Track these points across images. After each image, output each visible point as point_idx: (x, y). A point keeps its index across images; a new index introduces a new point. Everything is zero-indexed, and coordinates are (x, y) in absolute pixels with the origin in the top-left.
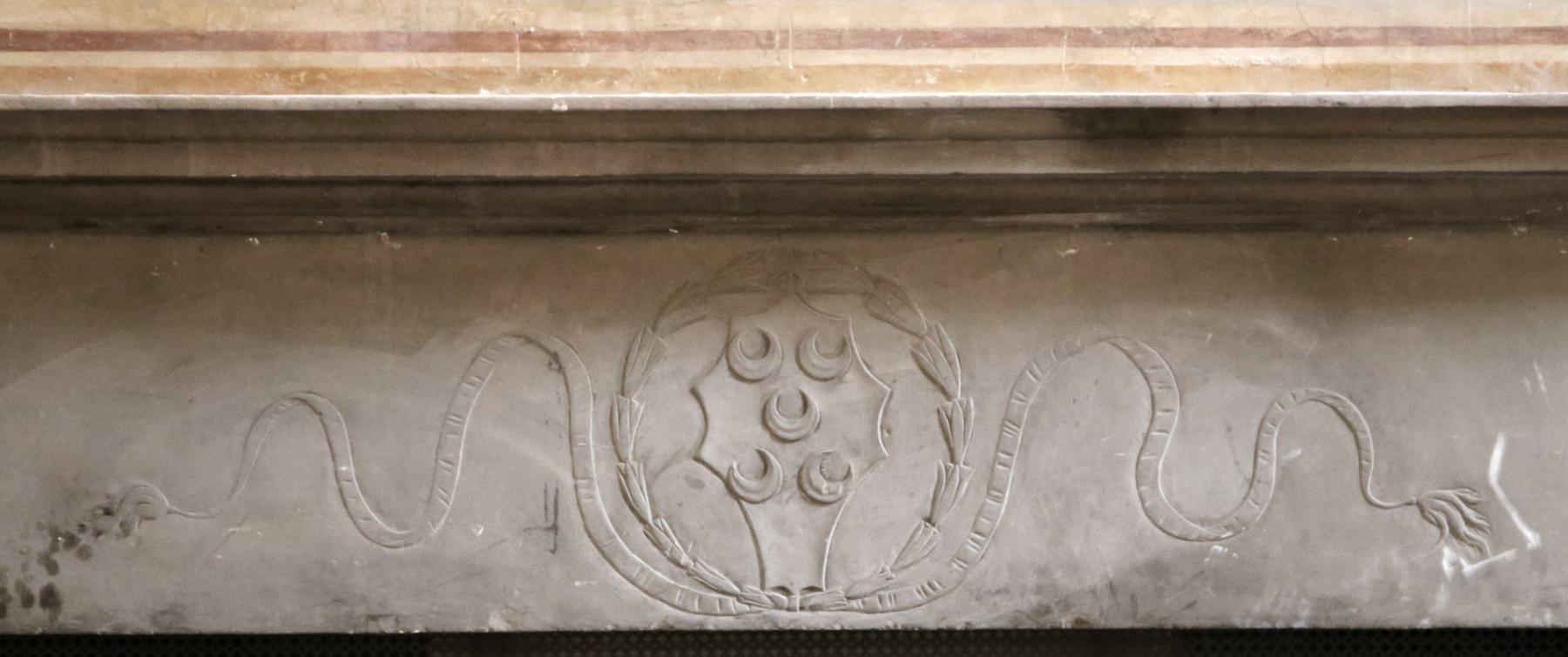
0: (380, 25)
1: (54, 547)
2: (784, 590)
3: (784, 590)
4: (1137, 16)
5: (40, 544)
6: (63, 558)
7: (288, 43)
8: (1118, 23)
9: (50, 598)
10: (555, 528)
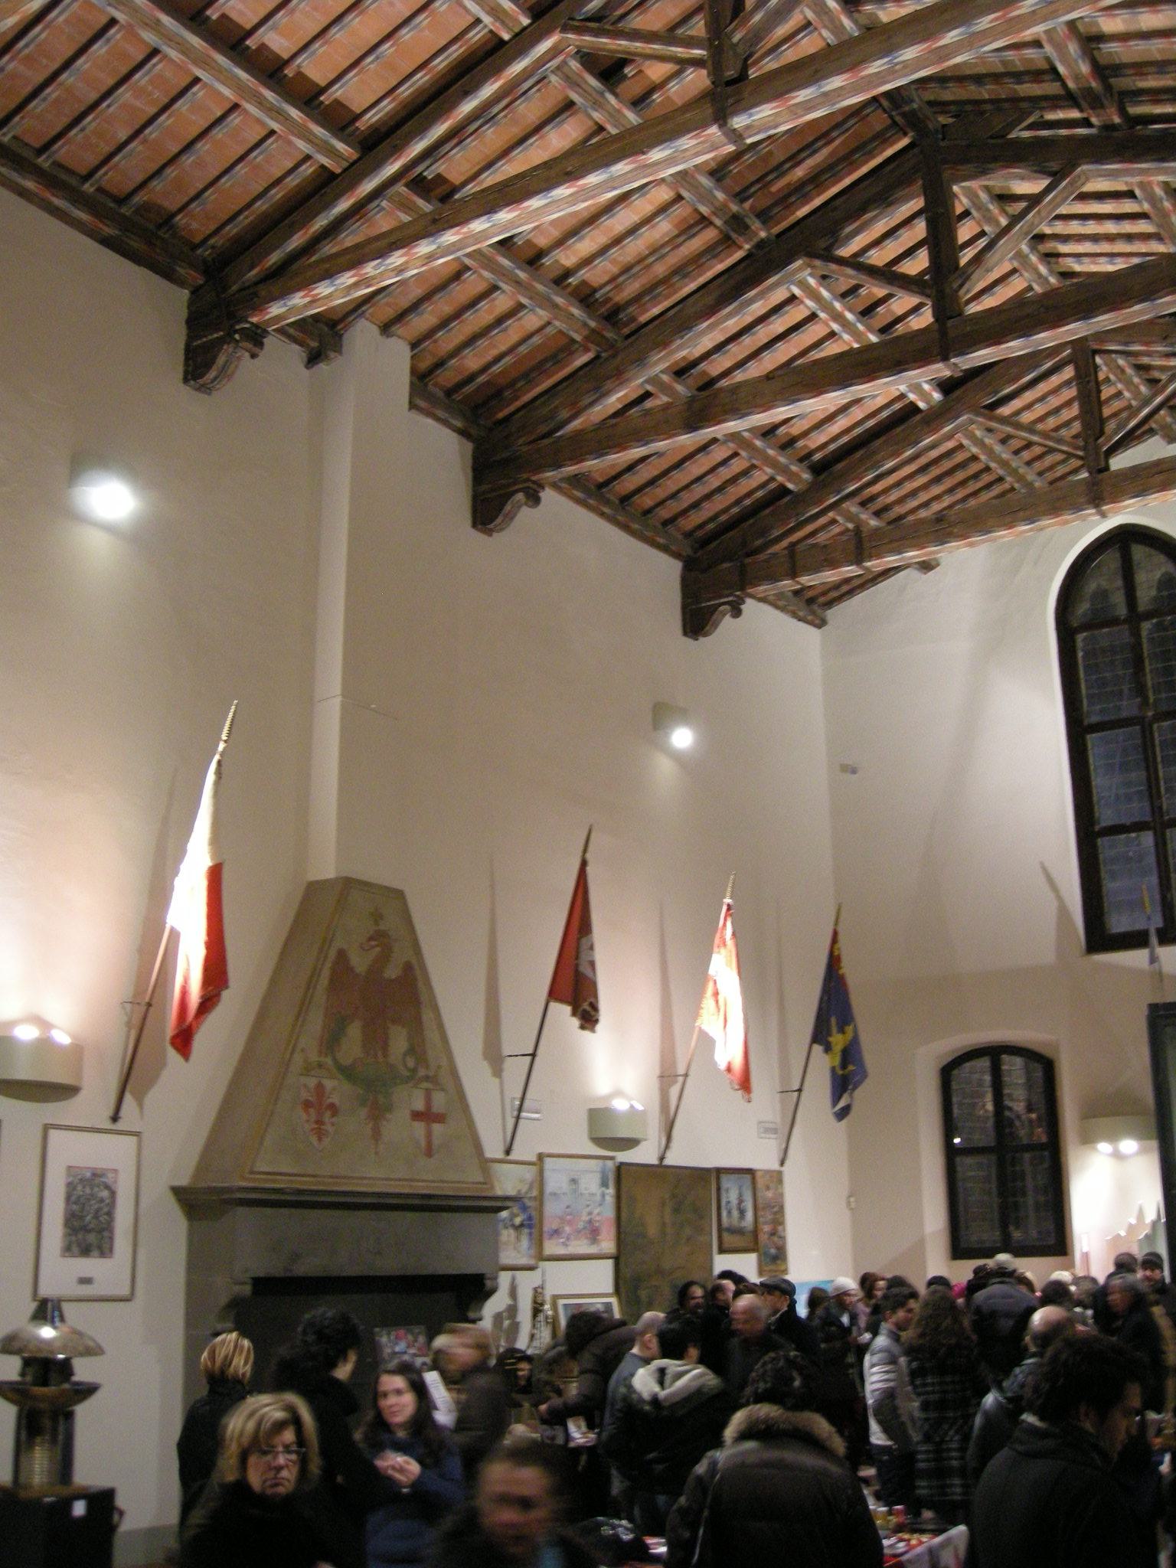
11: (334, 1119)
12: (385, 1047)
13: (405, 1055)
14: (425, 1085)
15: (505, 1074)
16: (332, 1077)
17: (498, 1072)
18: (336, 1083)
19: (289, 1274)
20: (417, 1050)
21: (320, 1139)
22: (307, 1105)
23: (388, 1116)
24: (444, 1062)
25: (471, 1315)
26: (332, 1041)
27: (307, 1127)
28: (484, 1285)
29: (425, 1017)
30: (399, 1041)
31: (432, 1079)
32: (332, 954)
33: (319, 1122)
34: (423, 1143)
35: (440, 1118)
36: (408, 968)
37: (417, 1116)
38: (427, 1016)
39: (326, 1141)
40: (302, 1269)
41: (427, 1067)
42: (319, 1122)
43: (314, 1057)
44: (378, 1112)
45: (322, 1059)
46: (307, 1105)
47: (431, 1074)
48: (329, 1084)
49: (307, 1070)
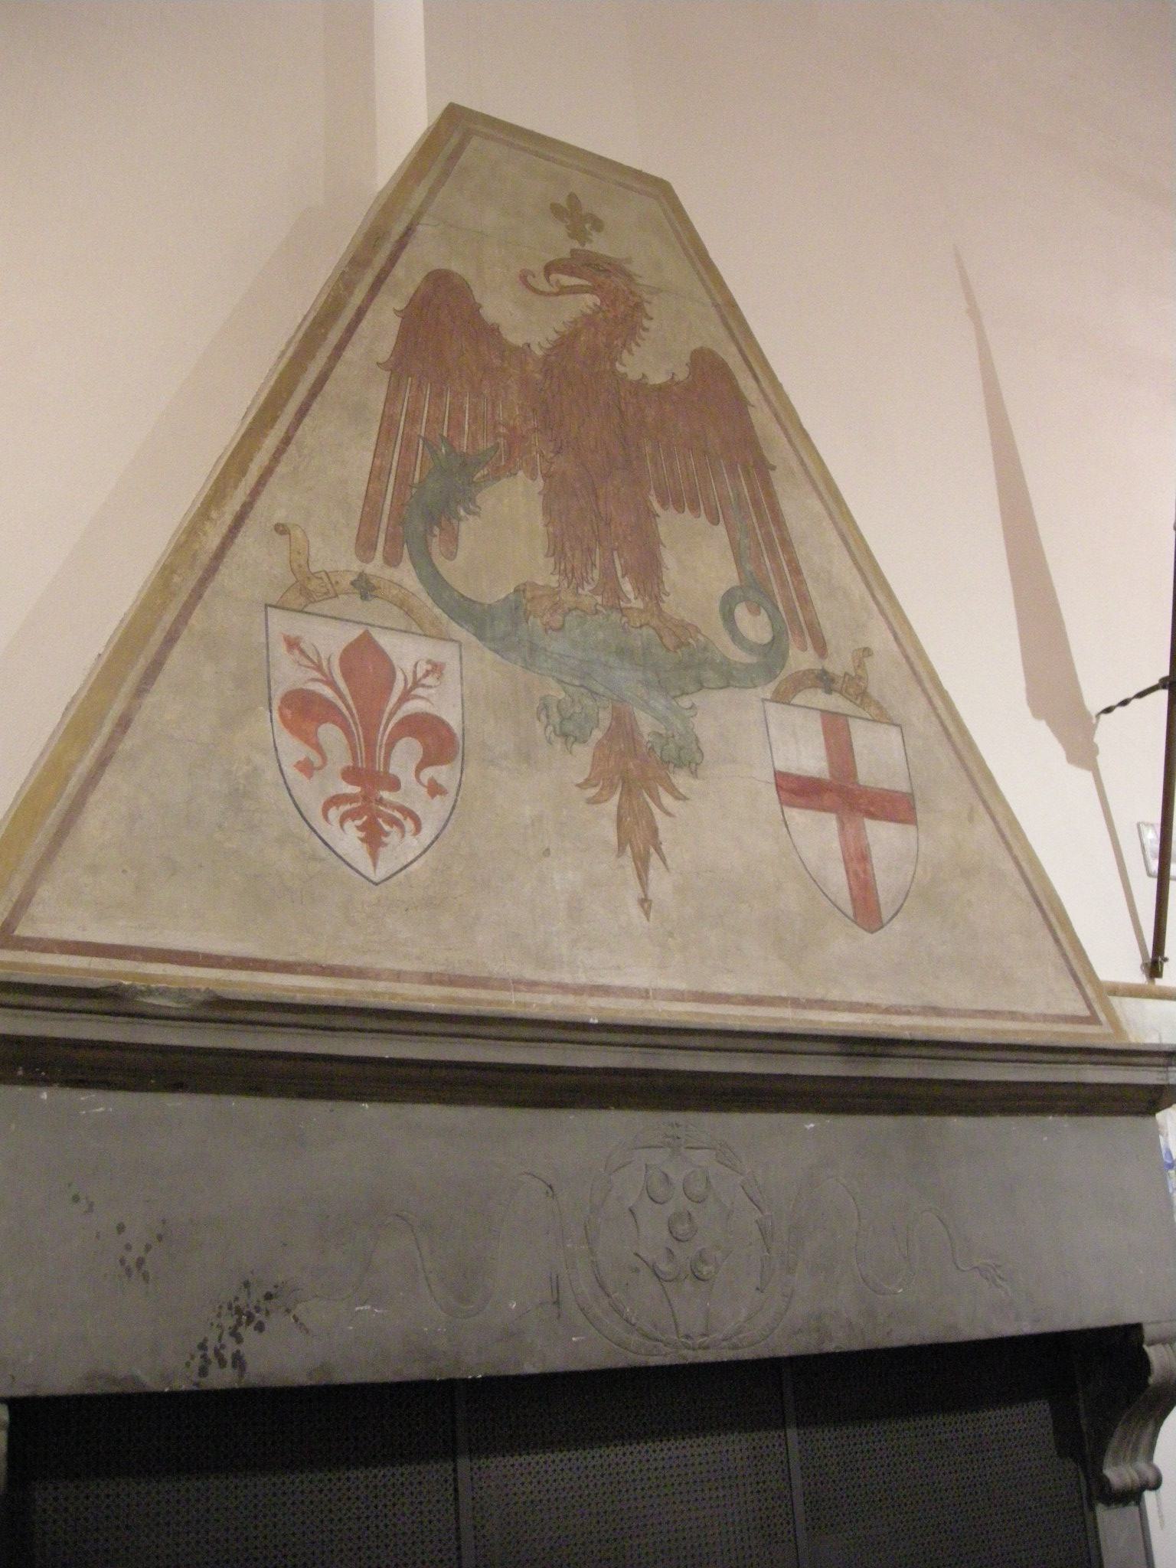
0: (432, 969)
1: (239, 1323)
2: (687, 1337)
3: (687, 1337)
4: (819, 993)
5: (229, 1322)
6: (248, 1332)
7: (377, 976)
8: (812, 996)
9: (238, 1361)
10: (557, 1303)
11: (441, 773)
12: (648, 571)
13: (728, 603)
14: (821, 699)
15: (1101, 760)
16: (416, 625)
17: (1082, 752)
18: (446, 653)
19: (222, 1378)
20: (770, 570)
21: (373, 838)
22: (303, 711)
23: (681, 780)
24: (879, 638)
25: (1117, 1474)
26: (417, 510)
27: (311, 794)
28: (1143, 1363)
29: (787, 507)
30: (698, 563)
31: (856, 687)
32: (408, 278)
33: (369, 774)
34: (837, 878)
35: (897, 807)
36: (708, 369)
37: (798, 790)
38: (799, 509)
39: (403, 847)
40: (280, 1357)
41: (821, 648)
42: (369, 774)
43: (334, 554)
44: (638, 773)
45: (375, 567)
46: (303, 711)
47: (839, 664)
48: (407, 653)
49: (305, 592)
